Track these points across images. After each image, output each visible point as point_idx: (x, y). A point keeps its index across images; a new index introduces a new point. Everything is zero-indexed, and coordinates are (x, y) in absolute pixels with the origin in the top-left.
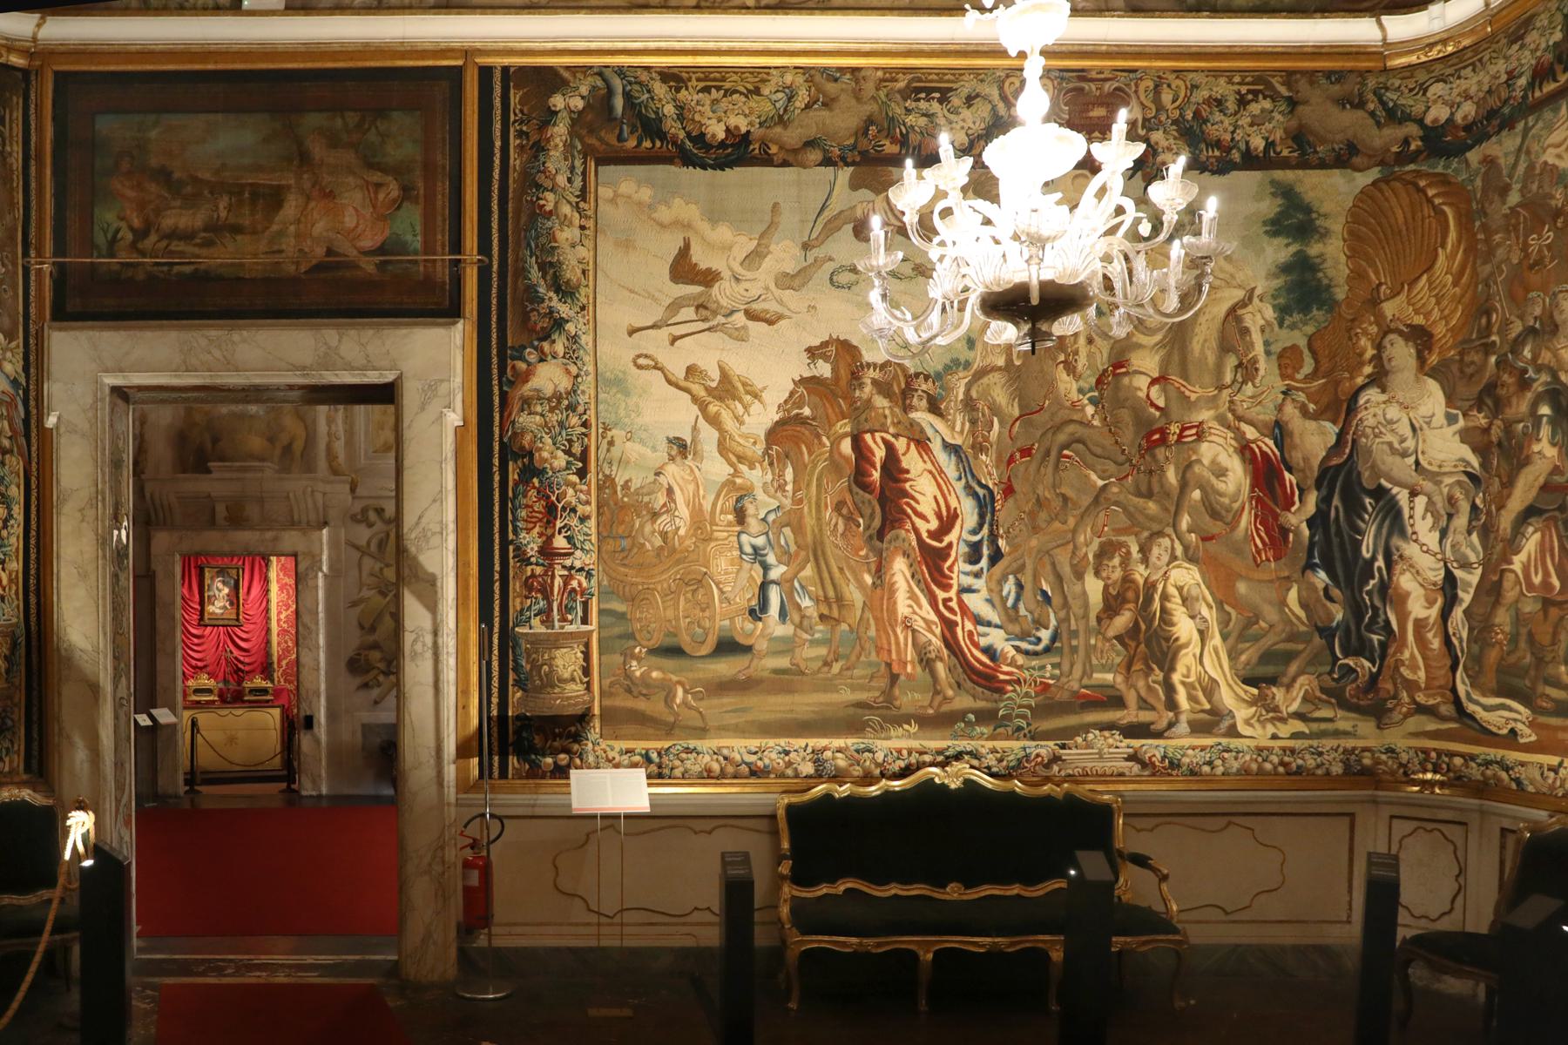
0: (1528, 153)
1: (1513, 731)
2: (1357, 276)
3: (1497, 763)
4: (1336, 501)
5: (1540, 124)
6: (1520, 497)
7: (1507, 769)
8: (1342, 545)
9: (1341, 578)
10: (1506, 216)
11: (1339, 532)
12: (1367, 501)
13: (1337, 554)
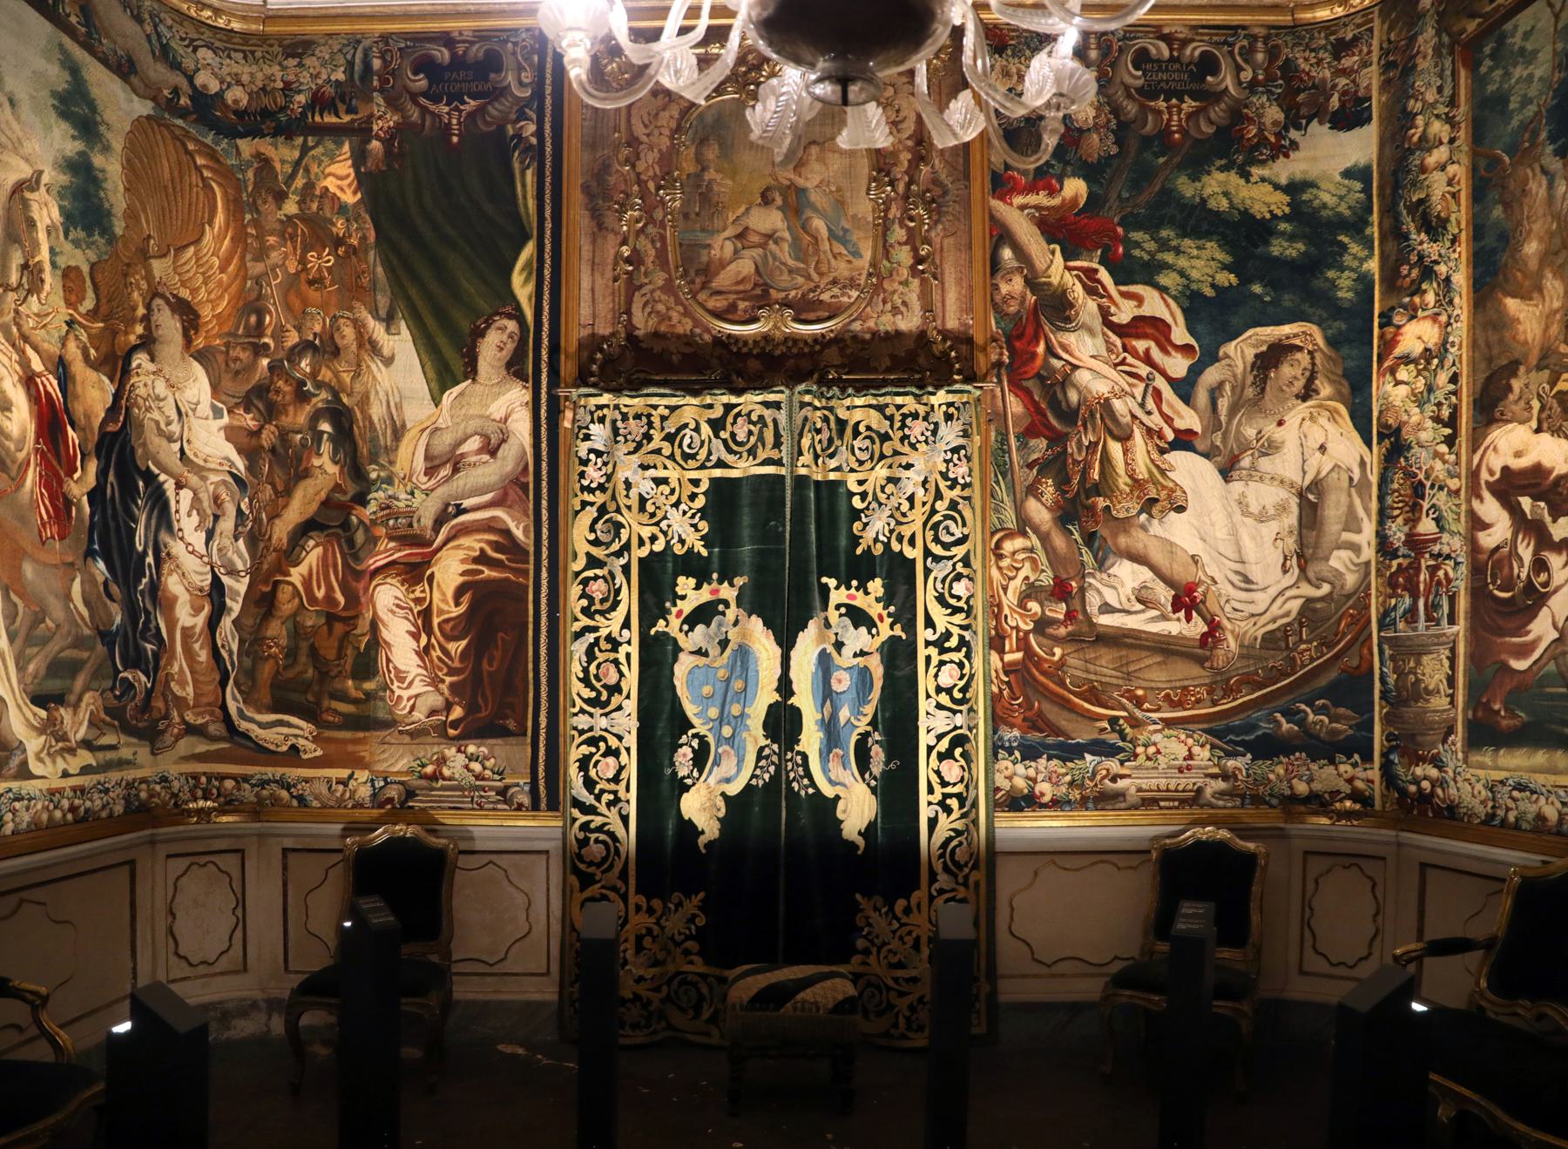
0: (307, 170)
1: (294, 748)
2: (131, 215)
3: (276, 782)
4: (111, 478)
5: (320, 150)
6: (297, 509)
7: (288, 787)
8: (118, 528)
9: (119, 573)
10: (281, 221)
11: (115, 517)
12: (141, 484)
13: (114, 543)
